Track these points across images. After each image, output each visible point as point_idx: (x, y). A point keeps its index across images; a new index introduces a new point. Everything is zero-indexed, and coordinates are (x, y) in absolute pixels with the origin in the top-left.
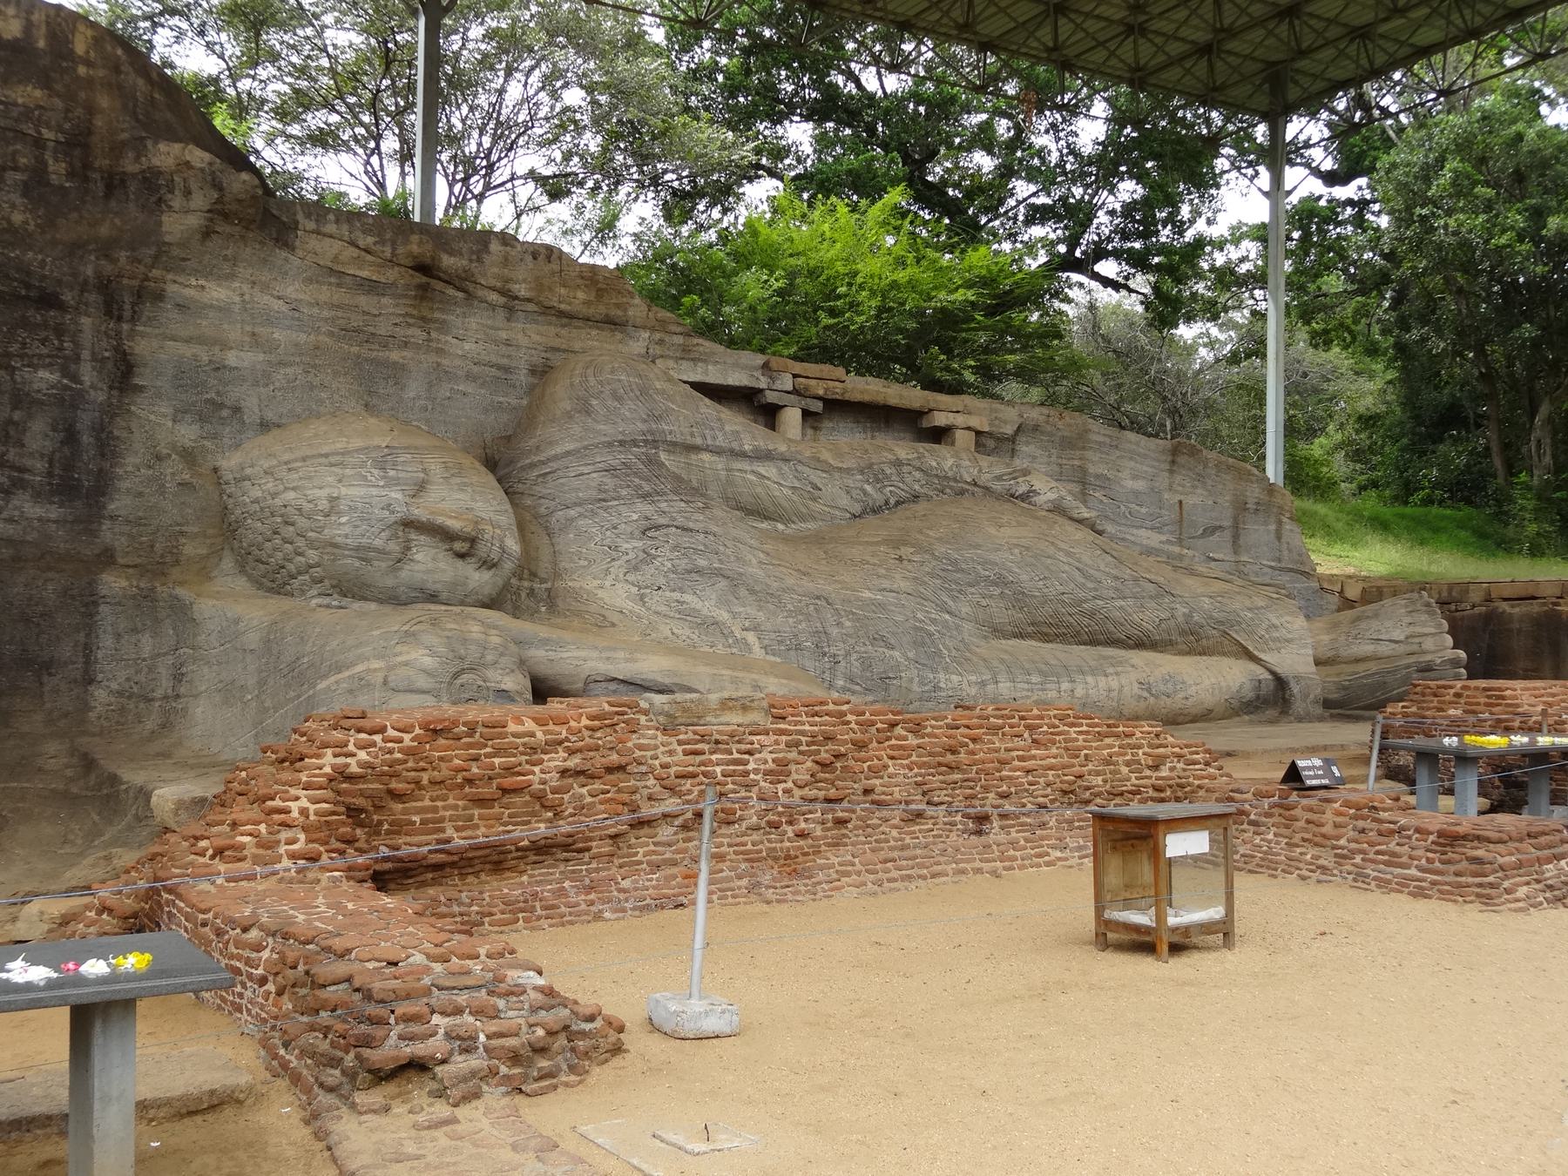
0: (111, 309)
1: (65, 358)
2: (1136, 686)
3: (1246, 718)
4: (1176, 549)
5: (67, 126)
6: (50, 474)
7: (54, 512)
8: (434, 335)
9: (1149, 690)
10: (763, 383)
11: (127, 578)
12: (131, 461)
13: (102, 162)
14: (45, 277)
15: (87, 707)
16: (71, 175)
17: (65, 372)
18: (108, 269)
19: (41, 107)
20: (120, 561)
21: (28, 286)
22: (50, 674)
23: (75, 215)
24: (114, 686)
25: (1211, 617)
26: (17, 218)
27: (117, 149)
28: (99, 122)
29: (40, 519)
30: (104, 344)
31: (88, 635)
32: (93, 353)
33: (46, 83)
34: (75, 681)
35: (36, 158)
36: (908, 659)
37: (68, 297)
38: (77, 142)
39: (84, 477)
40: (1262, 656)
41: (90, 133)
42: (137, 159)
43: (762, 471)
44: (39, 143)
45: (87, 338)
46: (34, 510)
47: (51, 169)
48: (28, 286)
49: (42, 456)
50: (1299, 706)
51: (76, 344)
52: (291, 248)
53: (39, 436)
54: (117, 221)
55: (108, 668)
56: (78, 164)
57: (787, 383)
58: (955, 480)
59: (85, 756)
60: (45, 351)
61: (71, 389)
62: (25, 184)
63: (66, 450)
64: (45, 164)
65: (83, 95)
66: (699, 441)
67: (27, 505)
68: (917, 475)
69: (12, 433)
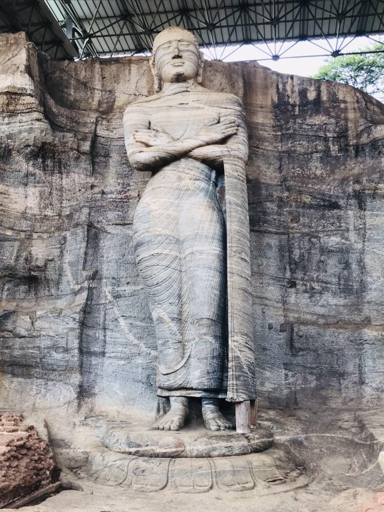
0: (361, 206)
1: (342, 230)
5: (337, 129)
6: (339, 284)
7: (342, 301)
11: (376, 331)
12: (375, 274)
13: (353, 142)
14: (331, 195)
15: (361, 397)
16: (340, 150)
17: (343, 237)
18: (357, 187)
19: (326, 124)
20: (373, 323)
21: (324, 201)
22: (344, 379)
23: (343, 167)
24: (374, 385)
26: (318, 172)
27: (359, 136)
28: (350, 125)
29: (336, 305)
30: (359, 222)
31: (360, 359)
32: (355, 227)
33: (328, 114)
34: (356, 383)
35: (325, 146)
37: (342, 202)
38: (342, 135)
39: (354, 284)
41: (347, 130)
42: (369, 135)
44: (326, 139)
45: (352, 220)
46: (333, 301)
47: (332, 149)
48: (324, 201)
49: (335, 276)
51: (347, 223)
53: (333, 265)
54: (361, 165)
55: (370, 376)
56: (343, 145)
59: (360, 422)
60: (333, 228)
61: (345, 244)
62: (321, 157)
63: (346, 272)
64: (329, 147)
65: (343, 115)
67: (330, 299)
69: (321, 266)
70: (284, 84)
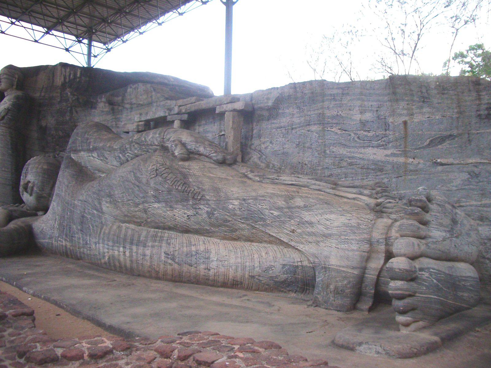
2: (163, 255)
3: (293, 295)
4: (402, 160)
8: (117, 122)
9: (173, 259)
10: (167, 114)
25: (235, 215)
36: (78, 230)
40: (300, 247)
43: (93, 155)
50: (319, 293)
52: (95, 108)
57: (176, 110)
58: (151, 145)
66: (81, 148)
68: (136, 146)
70: (66, 72)
